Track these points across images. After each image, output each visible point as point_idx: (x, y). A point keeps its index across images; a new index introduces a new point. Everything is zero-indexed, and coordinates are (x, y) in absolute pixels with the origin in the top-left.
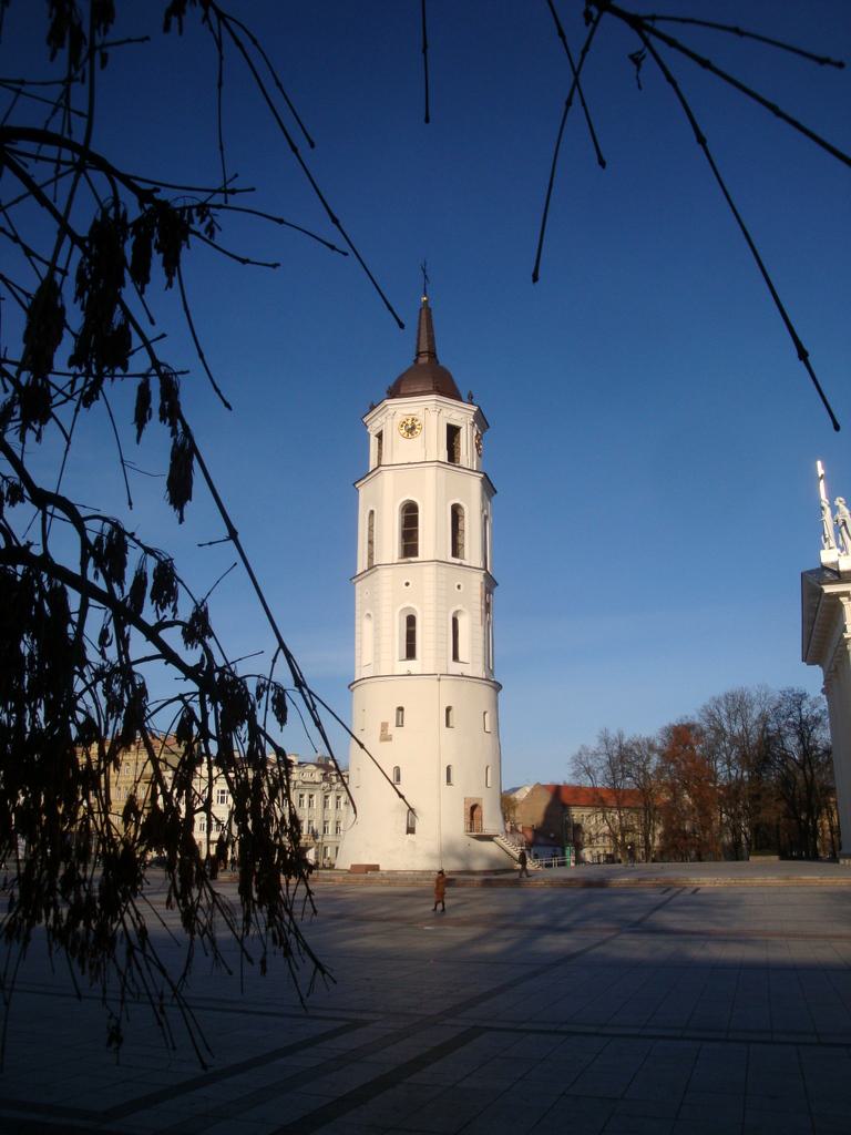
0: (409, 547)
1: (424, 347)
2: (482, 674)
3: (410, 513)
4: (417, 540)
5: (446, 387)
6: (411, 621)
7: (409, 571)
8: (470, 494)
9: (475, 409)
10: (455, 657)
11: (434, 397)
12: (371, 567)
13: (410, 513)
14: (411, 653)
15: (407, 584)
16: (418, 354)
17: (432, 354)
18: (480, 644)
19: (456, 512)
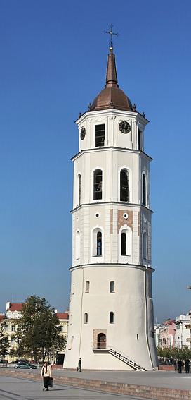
0: (98, 195)
1: (110, 78)
2: (137, 262)
3: (98, 176)
4: (94, 193)
5: (120, 103)
6: (99, 235)
7: (97, 209)
8: (133, 165)
9: (136, 114)
10: (123, 252)
11: (111, 110)
12: (80, 206)
13: (98, 176)
14: (99, 254)
15: (97, 215)
16: (107, 83)
17: (115, 82)
18: (138, 246)
19: (124, 176)
